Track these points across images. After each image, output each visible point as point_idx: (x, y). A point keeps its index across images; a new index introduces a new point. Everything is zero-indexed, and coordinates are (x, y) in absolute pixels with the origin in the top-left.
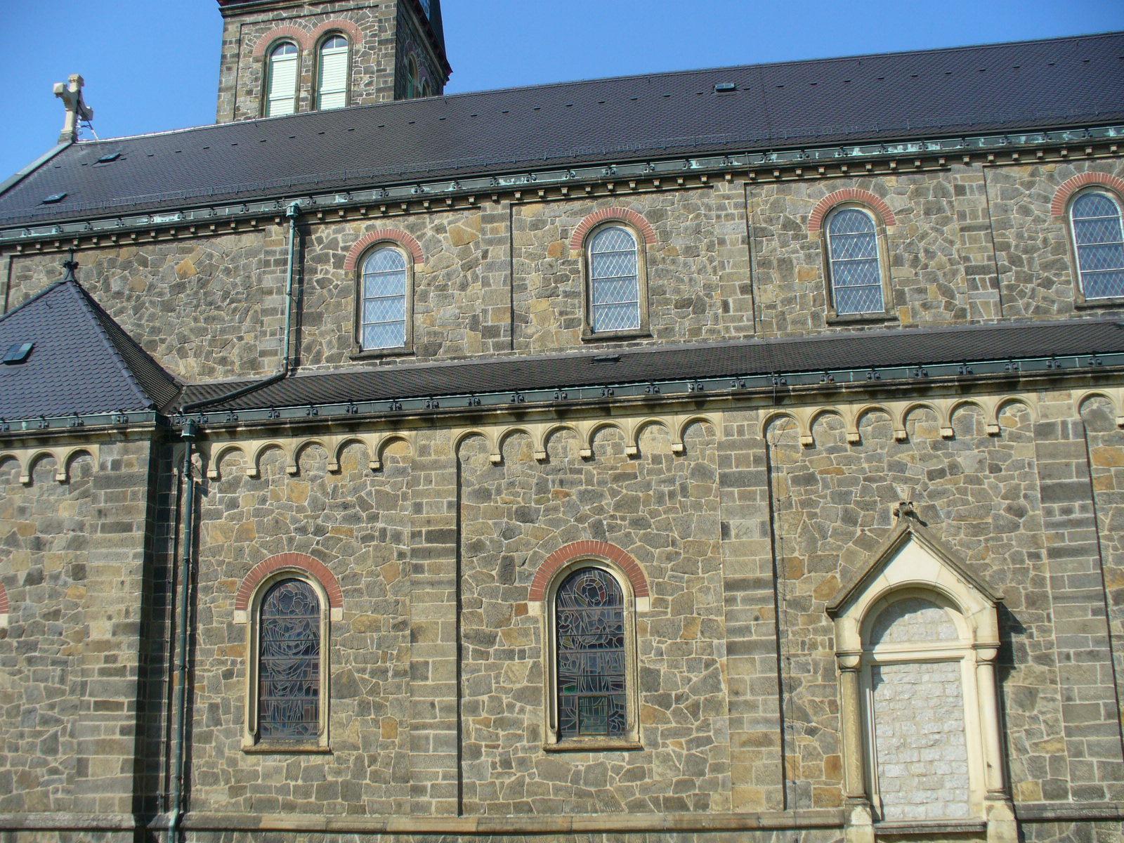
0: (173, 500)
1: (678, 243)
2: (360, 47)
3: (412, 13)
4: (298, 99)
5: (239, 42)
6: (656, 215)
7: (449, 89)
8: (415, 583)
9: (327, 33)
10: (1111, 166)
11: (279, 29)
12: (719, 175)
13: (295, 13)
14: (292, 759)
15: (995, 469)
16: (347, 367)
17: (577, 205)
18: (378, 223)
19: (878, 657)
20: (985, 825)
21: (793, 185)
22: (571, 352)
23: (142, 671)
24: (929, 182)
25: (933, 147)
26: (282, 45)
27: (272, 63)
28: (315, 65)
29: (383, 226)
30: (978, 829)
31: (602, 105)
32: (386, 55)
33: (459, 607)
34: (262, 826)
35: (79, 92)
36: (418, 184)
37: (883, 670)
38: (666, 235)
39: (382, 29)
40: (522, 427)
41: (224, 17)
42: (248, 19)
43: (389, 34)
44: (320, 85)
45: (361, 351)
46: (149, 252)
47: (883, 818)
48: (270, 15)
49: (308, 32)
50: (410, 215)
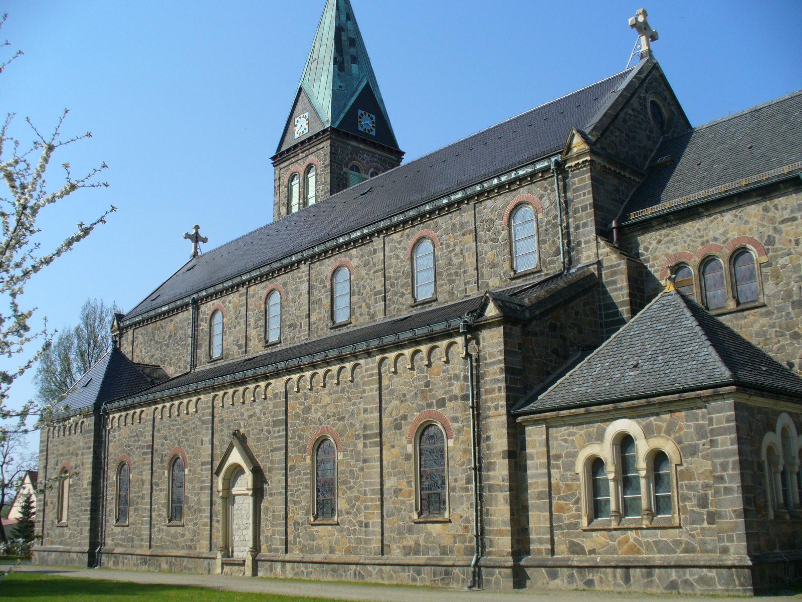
0: (104, 437)
1: (290, 296)
2: (319, 171)
3: (349, 142)
4: (299, 204)
5: (280, 178)
6: (285, 284)
7: (406, 160)
8: (144, 464)
9: (308, 166)
10: (430, 224)
11: (292, 168)
12: (299, 262)
13: (296, 158)
14: (122, 528)
15: (265, 414)
16: (330, 333)
17: (264, 284)
18: (215, 301)
19: (233, 493)
20: (244, 561)
21: (324, 261)
22: (260, 353)
23: (92, 498)
24: (367, 249)
25: (366, 231)
26: (294, 176)
27: (292, 186)
28: (304, 185)
29: (418, 231)
30: (242, 562)
31: (579, 108)
32: (327, 173)
33: (152, 473)
34: (114, 552)
35: (197, 233)
36: (498, 176)
37: (236, 498)
38: (287, 293)
39: (326, 160)
40: (344, 365)
41: (274, 166)
42: (282, 166)
43: (328, 162)
44: (307, 194)
45: (415, 302)
46: (163, 323)
47: (232, 556)
48: (289, 161)
49: (300, 168)
50: (415, 226)
